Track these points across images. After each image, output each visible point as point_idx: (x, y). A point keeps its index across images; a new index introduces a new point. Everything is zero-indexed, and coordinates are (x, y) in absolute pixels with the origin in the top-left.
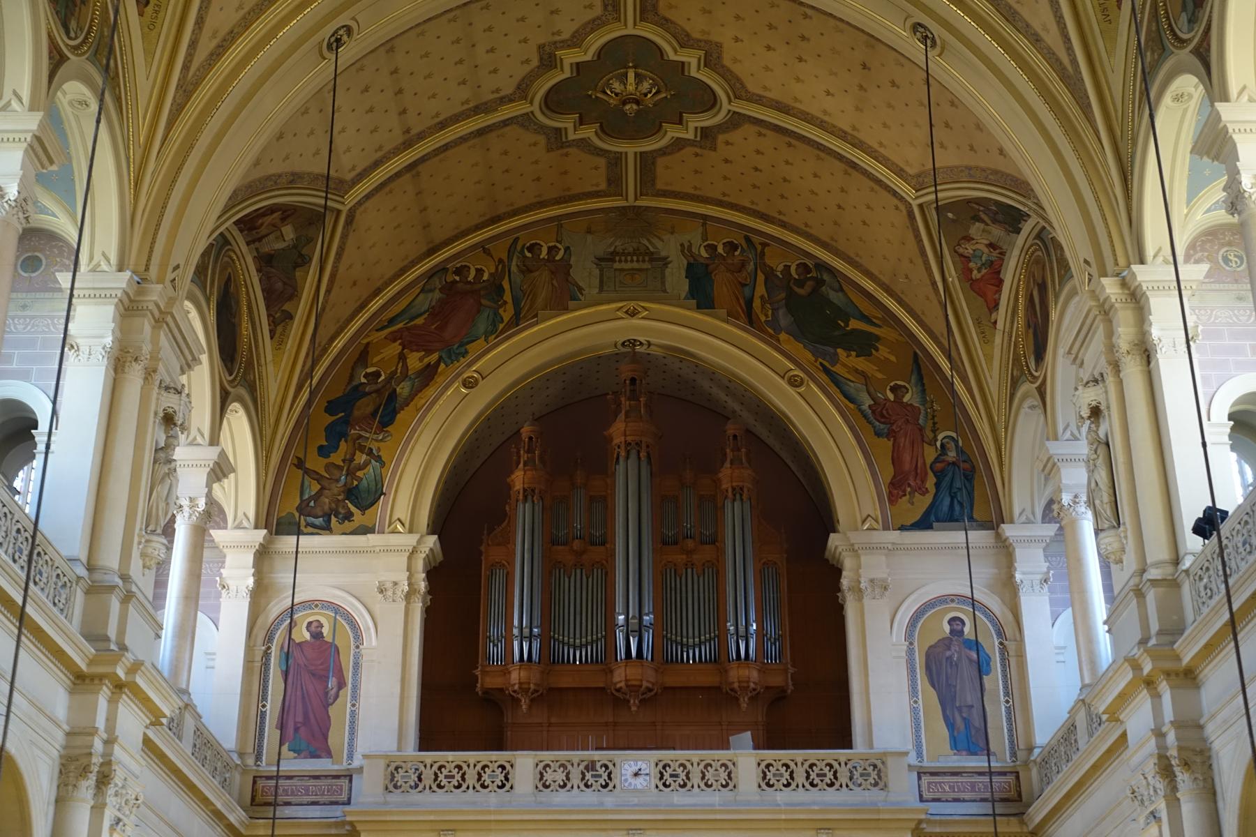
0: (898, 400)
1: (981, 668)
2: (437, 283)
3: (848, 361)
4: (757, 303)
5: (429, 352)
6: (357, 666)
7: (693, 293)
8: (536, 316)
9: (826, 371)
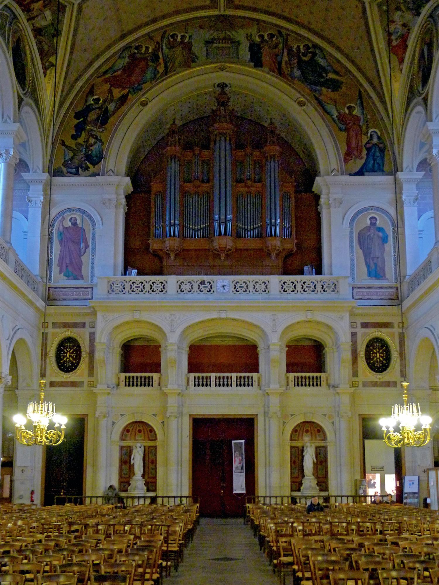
0: (350, 113)
1: (385, 240)
2: (127, 54)
5: (124, 88)
6: (94, 238)
7: (252, 60)
8: (175, 71)
9: (316, 99)
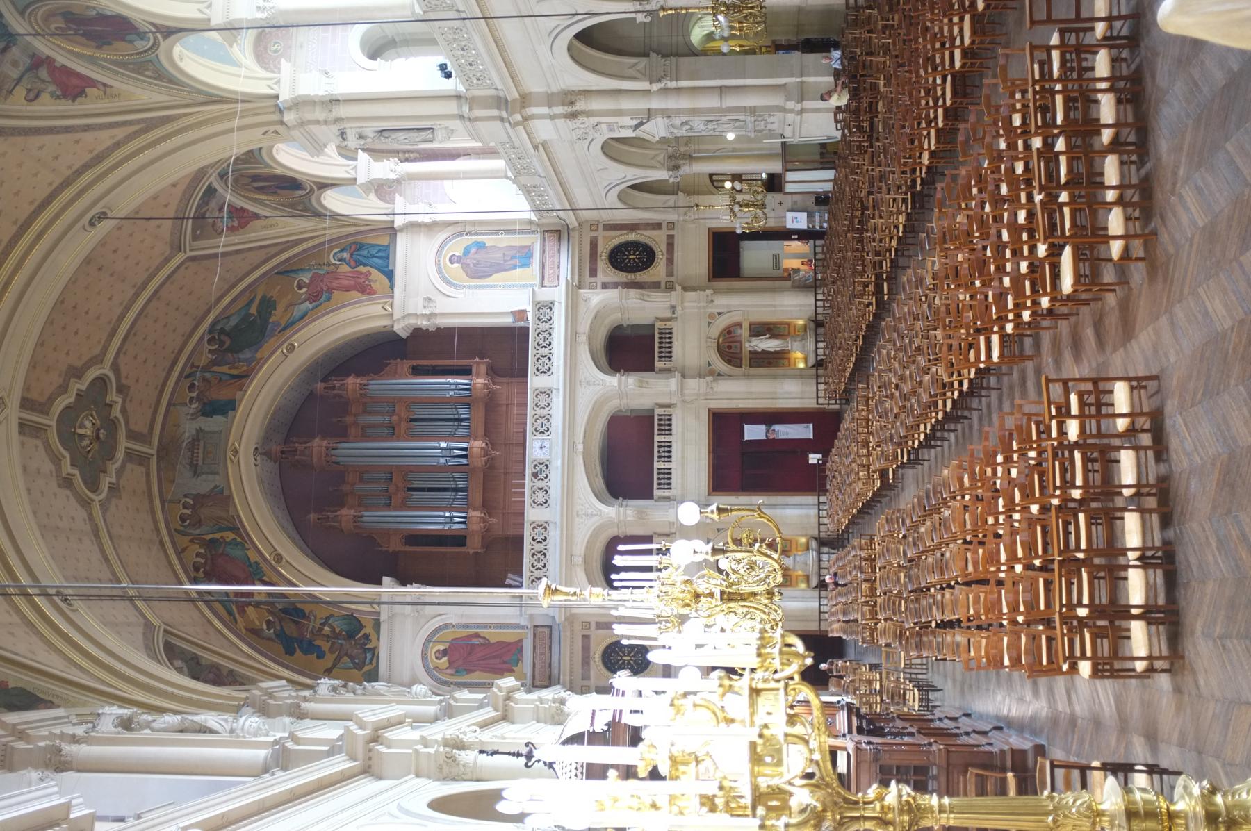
0: (307, 285)
3: (277, 316)
4: (234, 372)
6: (466, 626)
